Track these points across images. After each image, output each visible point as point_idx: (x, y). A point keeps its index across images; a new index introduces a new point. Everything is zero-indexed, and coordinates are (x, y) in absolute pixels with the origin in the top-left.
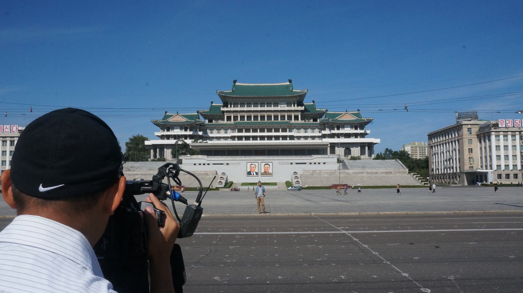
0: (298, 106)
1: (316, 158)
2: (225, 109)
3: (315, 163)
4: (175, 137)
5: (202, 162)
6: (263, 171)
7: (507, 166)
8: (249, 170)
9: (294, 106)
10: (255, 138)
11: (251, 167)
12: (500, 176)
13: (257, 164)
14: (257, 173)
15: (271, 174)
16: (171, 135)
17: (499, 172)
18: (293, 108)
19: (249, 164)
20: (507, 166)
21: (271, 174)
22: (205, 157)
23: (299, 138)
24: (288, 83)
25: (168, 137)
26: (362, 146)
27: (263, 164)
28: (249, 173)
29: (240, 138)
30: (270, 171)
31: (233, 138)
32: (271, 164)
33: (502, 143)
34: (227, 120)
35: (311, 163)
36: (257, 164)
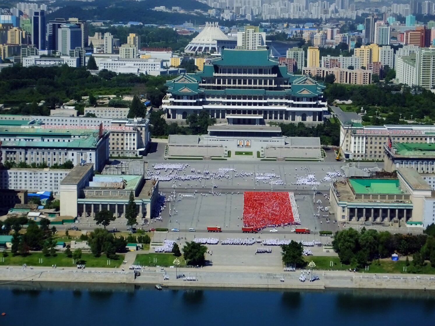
0: (272, 73)
1: (273, 138)
2: (217, 75)
5: (214, 139)
6: (246, 144)
7: (359, 152)
10: (239, 104)
12: (355, 156)
14: (242, 146)
16: (181, 102)
17: (355, 154)
19: (238, 141)
20: (359, 152)
21: (250, 146)
22: (216, 137)
23: (271, 104)
24: (266, 50)
26: (314, 114)
27: (246, 141)
28: (238, 145)
29: (229, 104)
30: (250, 145)
31: (224, 103)
32: (250, 141)
33: (357, 141)
34: (218, 83)
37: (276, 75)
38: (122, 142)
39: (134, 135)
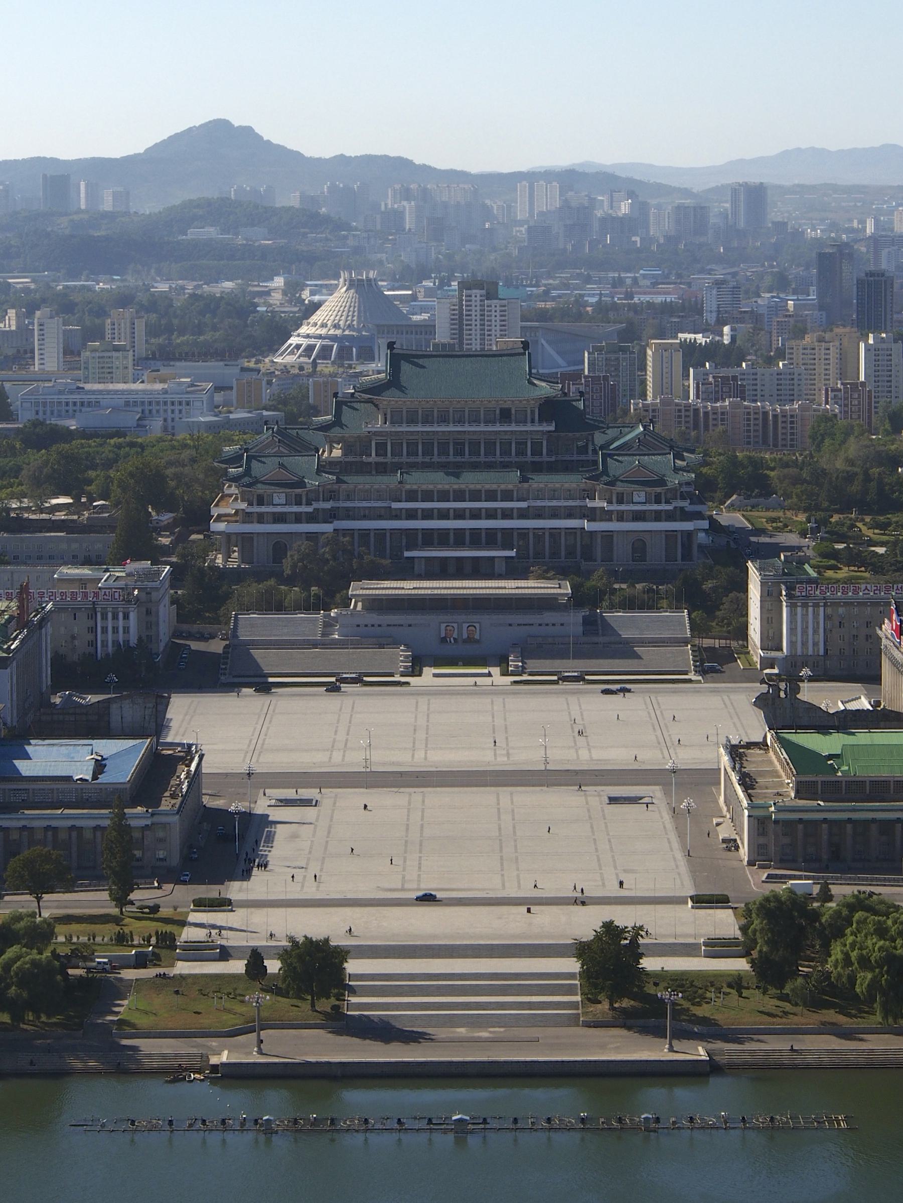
3: (547, 625)
4: (280, 518)
6: (465, 636)
8: (443, 635)
9: (533, 421)
11: (446, 630)
13: (455, 625)
15: (478, 641)
18: (529, 428)
19: (443, 626)
25: (261, 518)
27: (465, 626)
28: (444, 640)
30: (477, 637)
32: (477, 625)
35: (540, 625)
36: (455, 625)
37: (552, 428)
38: (91, 637)
39: (126, 617)
